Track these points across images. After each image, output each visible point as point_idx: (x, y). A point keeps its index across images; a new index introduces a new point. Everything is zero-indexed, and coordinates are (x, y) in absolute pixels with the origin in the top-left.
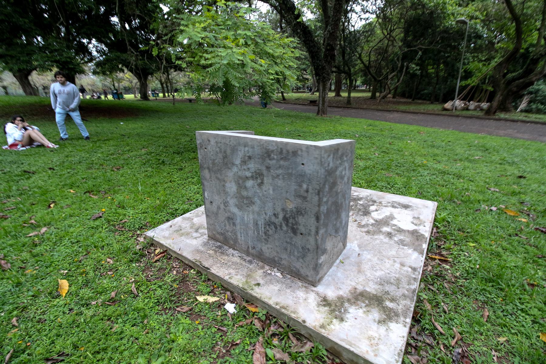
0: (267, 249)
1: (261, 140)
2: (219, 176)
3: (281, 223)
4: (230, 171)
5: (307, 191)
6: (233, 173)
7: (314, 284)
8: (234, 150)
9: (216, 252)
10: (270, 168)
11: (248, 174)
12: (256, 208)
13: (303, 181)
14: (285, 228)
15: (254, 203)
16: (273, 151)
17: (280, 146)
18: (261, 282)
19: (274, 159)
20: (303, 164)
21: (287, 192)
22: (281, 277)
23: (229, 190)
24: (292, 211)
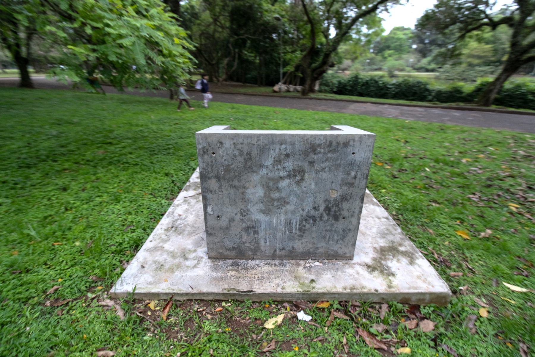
0: (299, 246)
1: (305, 135)
2: (236, 183)
3: (322, 214)
4: (255, 174)
5: (355, 177)
6: (260, 176)
7: (351, 258)
8: (263, 150)
9: (237, 270)
10: (314, 162)
11: (282, 173)
12: (290, 208)
13: (352, 169)
14: (325, 217)
15: (288, 203)
16: (319, 145)
17: (329, 139)
18: (313, 277)
19: (320, 152)
20: (353, 153)
21: (332, 182)
22: (321, 264)
23: (251, 197)
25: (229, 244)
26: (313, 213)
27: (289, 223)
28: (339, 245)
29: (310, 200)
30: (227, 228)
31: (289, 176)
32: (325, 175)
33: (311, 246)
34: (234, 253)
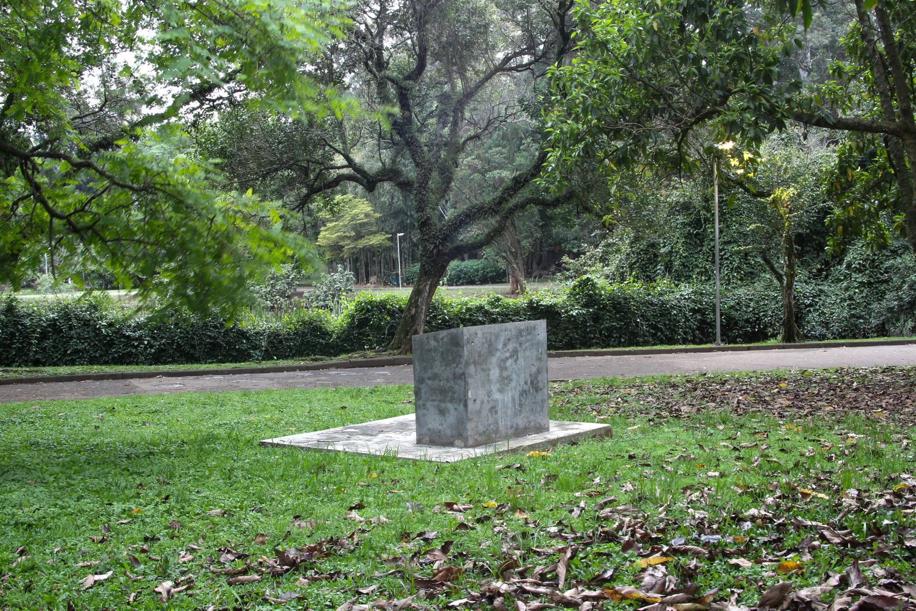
0: (521, 422)
2: (484, 367)
8: (497, 336)
12: (513, 384)
26: (526, 388)
29: (522, 375)
31: (511, 356)
32: (528, 353)
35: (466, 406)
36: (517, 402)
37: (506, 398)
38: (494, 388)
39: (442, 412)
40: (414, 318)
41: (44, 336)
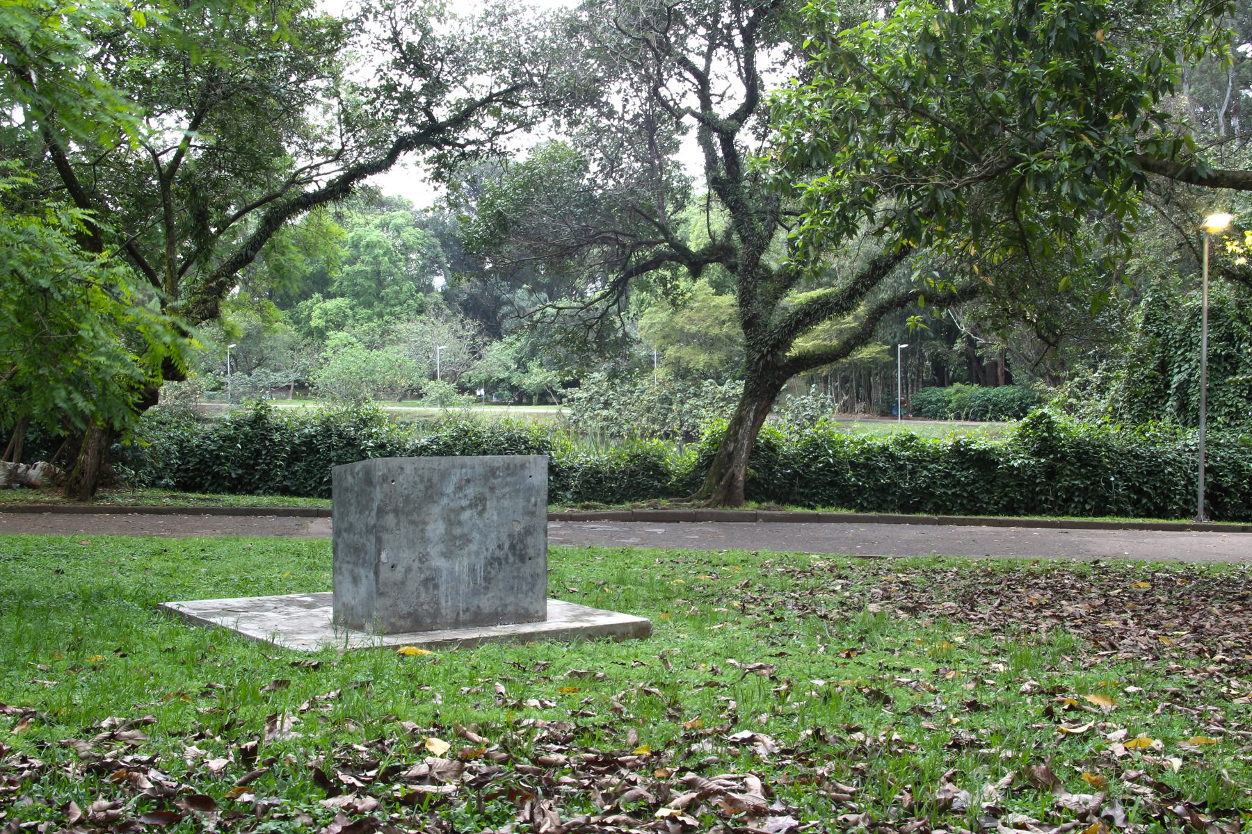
0: (486, 603)
2: (415, 517)
5: (535, 505)
8: (445, 475)
11: (465, 503)
12: (473, 547)
14: (511, 559)
15: (471, 541)
16: (498, 468)
24: (519, 534)
25: (404, 608)
26: (498, 553)
27: (472, 570)
28: (529, 600)
29: (494, 535)
30: (403, 583)
31: (471, 506)
32: (506, 503)
33: (498, 603)
34: (408, 623)
35: (377, 573)
36: (480, 573)
37: (456, 568)
38: (434, 551)
39: (356, 580)
40: (730, 456)
41: (295, 456)
